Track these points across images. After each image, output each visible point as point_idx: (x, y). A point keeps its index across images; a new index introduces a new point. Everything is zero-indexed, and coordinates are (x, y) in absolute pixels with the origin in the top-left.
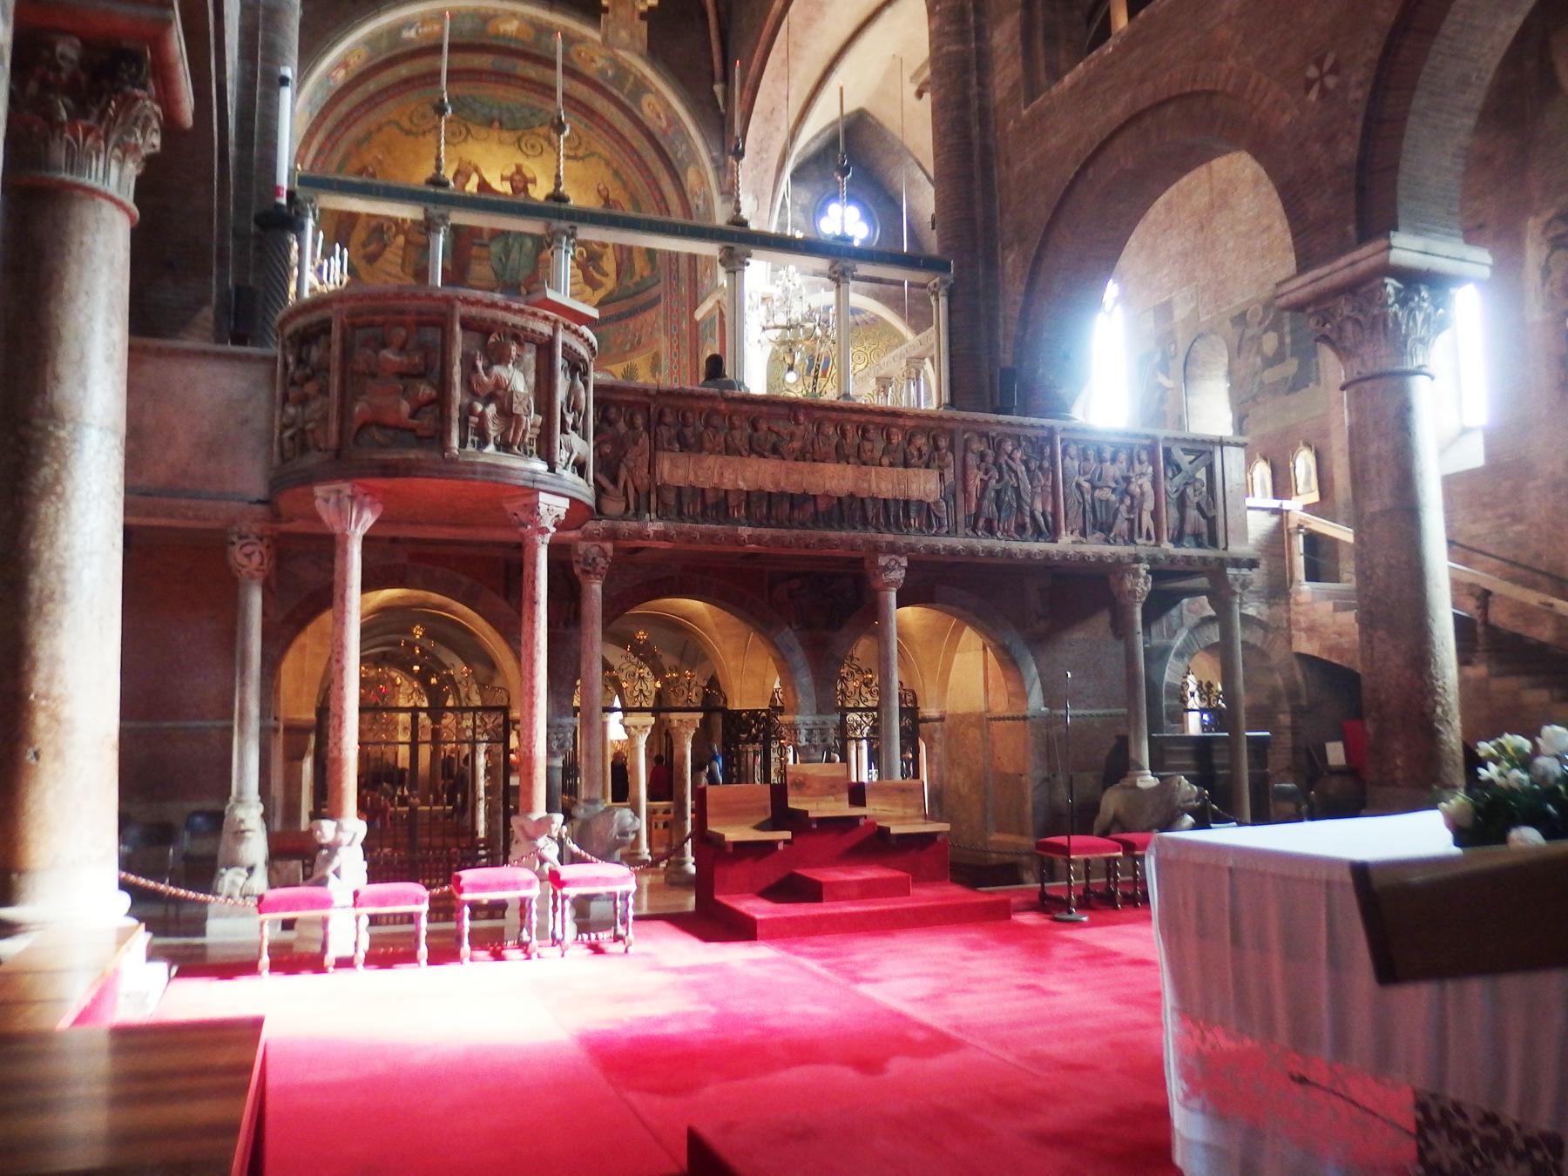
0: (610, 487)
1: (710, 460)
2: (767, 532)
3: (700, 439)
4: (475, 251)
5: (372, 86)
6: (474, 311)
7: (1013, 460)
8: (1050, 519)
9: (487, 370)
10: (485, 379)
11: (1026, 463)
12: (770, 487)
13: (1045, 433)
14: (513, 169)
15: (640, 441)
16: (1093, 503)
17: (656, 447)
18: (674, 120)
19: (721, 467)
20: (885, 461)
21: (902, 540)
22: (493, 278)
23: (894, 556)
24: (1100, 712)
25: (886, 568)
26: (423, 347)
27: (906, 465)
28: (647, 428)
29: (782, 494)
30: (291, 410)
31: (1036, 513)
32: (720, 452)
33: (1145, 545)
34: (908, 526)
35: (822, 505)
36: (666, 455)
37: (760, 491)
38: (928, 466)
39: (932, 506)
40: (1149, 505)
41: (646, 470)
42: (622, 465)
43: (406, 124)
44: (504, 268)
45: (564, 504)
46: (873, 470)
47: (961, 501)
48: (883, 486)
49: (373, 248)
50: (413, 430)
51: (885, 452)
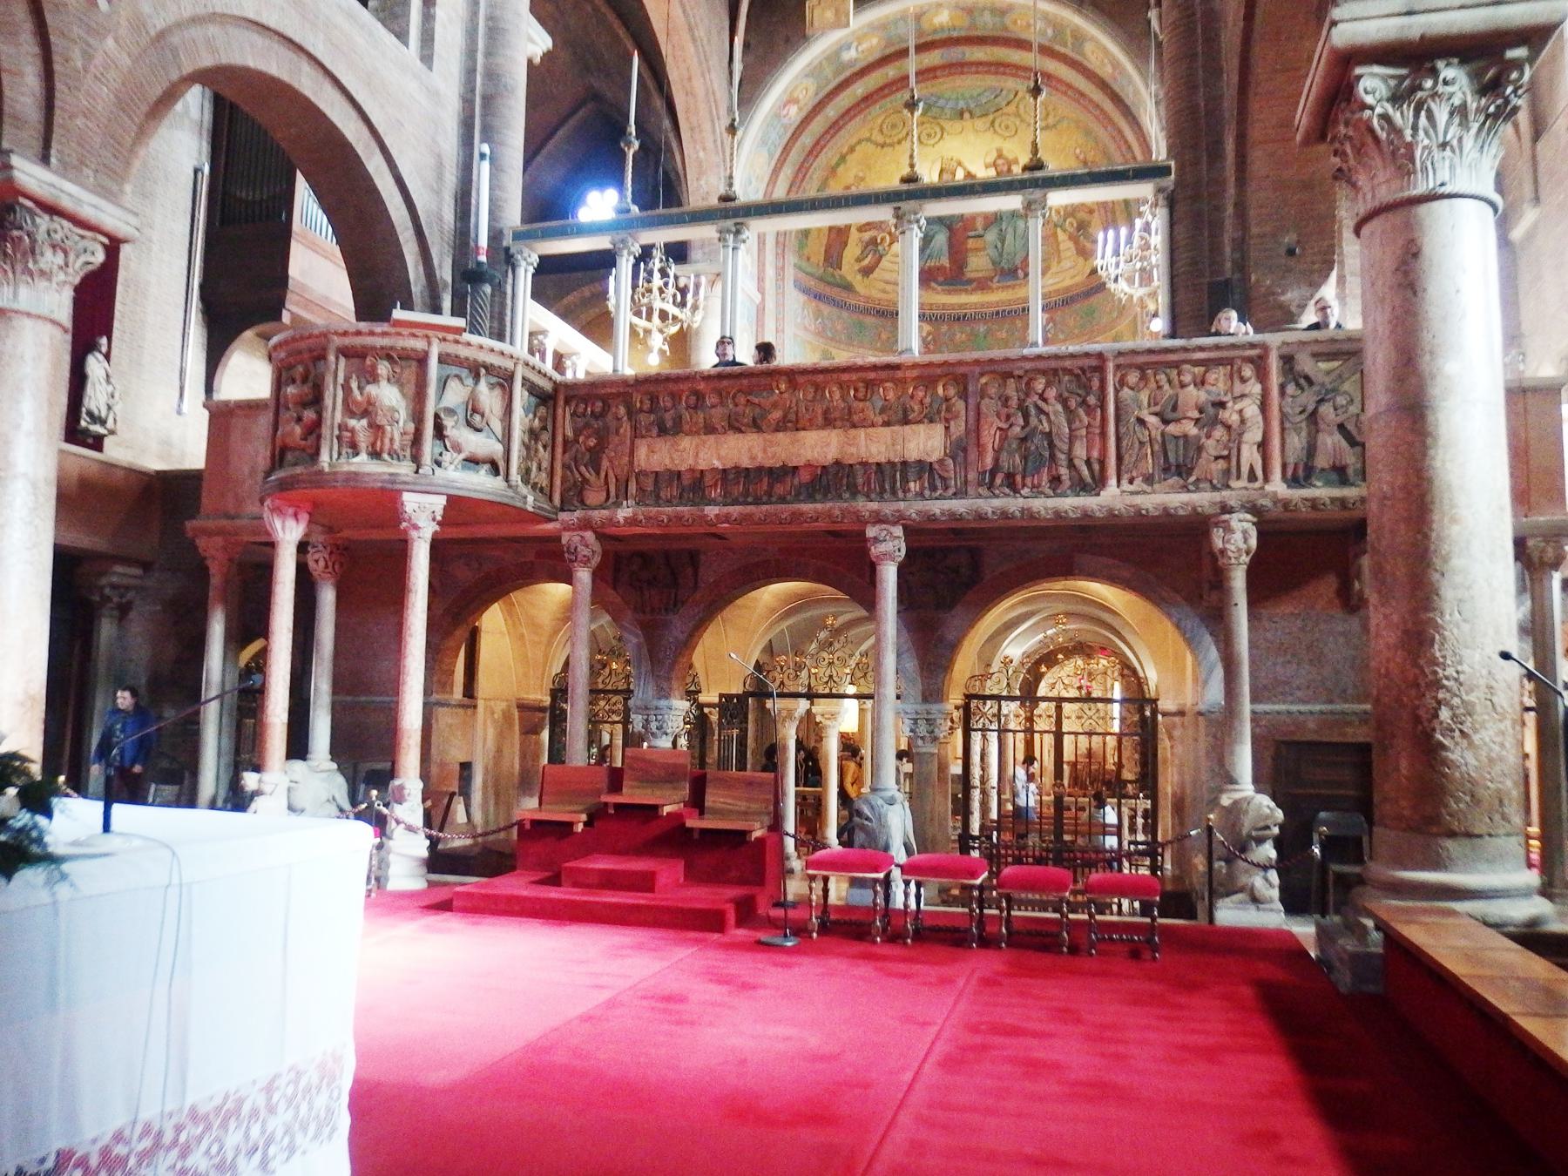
0: (590, 475)
1: (686, 443)
2: (735, 510)
3: (678, 421)
4: (971, 243)
5: (831, 112)
6: (347, 341)
7: (1045, 400)
8: (1096, 467)
9: (360, 388)
10: (359, 398)
11: (1064, 402)
12: (746, 463)
13: (1087, 362)
14: (995, 155)
15: (622, 431)
16: (1164, 443)
17: (636, 434)
18: (1116, 65)
19: (697, 446)
20: (879, 420)
21: (888, 508)
22: (990, 266)
23: (884, 526)
24: (1317, 708)
25: (876, 540)
27: (906, 421)
29: (760, 469)
31: (1077, 462)
32: (697, 433)
33: (1246, 488)
34: (906, 491)
35: (805, 477)
36: (644, 441)
37: (737, 469)
38: (931, 421)
39: (936, 466)
40: (1254, 435)
43: (880, 139)
44: (1001, 255)
45: (442, 500)
46: (862, 433)
47: (973, 456)
48: (874, 450)
49: (866, 262)
51: (883, 411)
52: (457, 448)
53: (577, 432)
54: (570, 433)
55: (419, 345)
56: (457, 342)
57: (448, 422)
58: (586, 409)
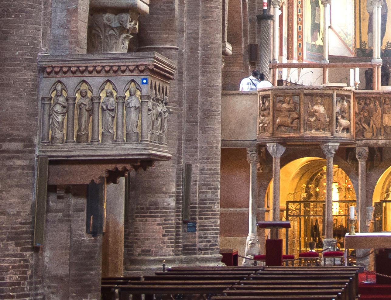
6: (308, 91)
10: (312, 110)
15: (378, 111)
17: (383, 112)
26: (294, 102)
28: (381, 107)
30: (261, 118)
36: (386, 115)
41: (380, 121)
42: (371, 120)
50: (292, 127)
52: (341, 126)
53: (360, 111)
54: (357, 111)
55: (330, 92)
56: (341, 90)
57: (339, 117)
58: (363, 102)
